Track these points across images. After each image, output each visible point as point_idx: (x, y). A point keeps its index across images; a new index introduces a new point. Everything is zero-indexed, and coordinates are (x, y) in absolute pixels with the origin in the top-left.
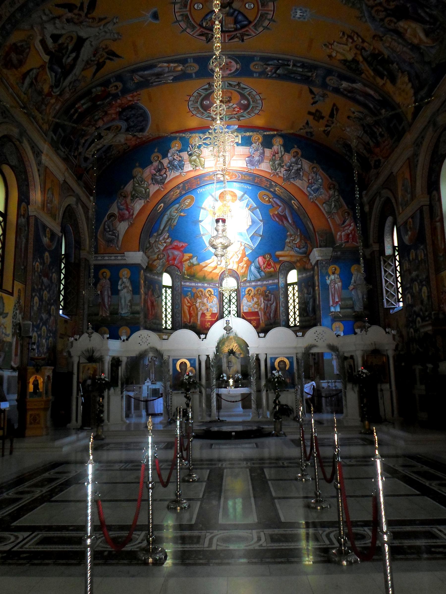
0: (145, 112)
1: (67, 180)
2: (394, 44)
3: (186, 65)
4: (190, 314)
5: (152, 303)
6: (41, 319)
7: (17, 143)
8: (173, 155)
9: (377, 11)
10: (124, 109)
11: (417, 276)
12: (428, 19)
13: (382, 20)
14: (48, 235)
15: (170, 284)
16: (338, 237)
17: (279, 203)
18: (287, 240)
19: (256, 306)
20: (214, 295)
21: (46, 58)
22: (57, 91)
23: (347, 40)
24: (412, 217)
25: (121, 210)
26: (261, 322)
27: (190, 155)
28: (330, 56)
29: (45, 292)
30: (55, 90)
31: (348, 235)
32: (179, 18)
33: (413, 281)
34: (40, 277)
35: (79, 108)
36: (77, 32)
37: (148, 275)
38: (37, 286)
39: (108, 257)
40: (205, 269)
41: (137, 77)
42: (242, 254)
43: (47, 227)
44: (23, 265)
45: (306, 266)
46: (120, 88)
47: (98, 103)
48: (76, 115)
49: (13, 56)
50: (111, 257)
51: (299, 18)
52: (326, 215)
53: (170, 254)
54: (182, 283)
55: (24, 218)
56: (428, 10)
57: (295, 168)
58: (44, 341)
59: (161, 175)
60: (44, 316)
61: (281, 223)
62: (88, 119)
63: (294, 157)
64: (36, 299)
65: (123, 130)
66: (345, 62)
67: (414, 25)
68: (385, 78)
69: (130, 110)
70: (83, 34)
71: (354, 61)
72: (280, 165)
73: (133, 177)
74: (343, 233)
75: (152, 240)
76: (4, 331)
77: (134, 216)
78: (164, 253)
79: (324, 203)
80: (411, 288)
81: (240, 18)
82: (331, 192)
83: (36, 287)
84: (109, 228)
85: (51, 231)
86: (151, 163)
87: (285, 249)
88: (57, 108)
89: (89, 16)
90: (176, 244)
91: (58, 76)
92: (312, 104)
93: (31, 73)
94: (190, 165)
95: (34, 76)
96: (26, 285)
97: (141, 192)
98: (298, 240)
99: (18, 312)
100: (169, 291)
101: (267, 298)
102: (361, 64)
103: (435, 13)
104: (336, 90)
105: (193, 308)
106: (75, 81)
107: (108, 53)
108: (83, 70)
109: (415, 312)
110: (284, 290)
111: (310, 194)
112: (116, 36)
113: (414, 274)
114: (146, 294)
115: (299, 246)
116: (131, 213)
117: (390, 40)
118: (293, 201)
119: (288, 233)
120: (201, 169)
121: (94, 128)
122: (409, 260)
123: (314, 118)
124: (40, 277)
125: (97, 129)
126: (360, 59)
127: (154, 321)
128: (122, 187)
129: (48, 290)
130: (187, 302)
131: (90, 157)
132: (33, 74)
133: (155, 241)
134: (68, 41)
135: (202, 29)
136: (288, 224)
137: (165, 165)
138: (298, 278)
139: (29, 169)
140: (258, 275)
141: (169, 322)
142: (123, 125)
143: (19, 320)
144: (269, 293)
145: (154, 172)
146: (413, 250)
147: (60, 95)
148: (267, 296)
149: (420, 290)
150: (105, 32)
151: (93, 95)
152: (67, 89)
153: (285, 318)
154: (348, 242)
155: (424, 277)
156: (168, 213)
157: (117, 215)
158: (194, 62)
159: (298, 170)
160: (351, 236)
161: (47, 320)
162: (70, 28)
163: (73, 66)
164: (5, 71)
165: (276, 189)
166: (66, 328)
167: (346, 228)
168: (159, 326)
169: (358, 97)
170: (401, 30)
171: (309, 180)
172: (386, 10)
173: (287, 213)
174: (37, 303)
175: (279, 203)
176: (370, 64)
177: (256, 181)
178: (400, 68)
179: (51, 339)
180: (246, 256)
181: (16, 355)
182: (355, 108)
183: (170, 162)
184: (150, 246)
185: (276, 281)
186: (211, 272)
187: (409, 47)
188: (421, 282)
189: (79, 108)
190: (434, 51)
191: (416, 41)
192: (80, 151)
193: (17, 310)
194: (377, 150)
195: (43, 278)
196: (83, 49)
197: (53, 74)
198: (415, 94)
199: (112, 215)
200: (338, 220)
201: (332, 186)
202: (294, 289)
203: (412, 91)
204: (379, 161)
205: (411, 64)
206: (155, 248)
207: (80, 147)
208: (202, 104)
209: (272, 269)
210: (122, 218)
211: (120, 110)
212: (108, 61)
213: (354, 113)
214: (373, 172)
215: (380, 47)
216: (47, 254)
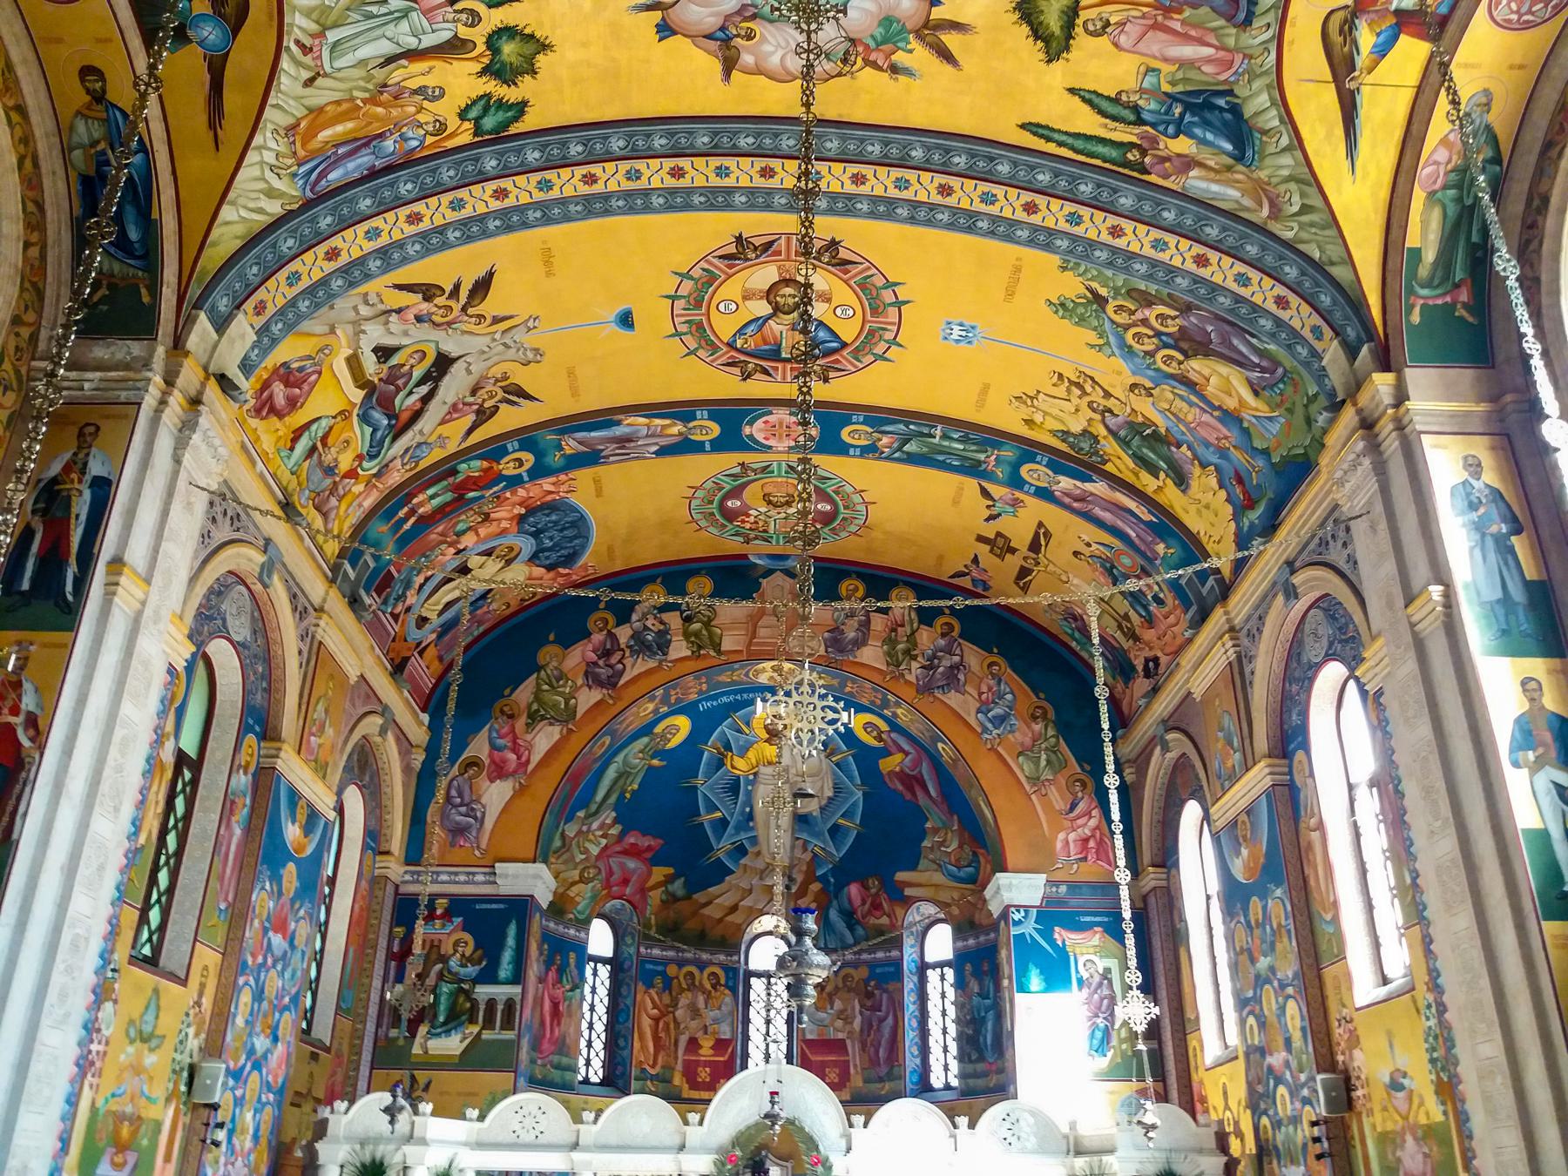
0: (582, 518)
1: (368, 676)
2: (1178, 403)
3: (691, 425)
4: (656, 1039)
5: (555, 1005)
6: (251, 1052)
7: (258, 587)
8: (644, 617)
9: (1138, 337)
10: (531, 511)
11: (1272, 969)
12: (1256, 360)
13: (1151, 354)
14: (302, 815)
15: (608, 951)
16: (1059, 845)
17: (906, 747)
18: (926, 843)
19: (839, 1023)
20: (726, 986)
21: (357, 395)
22: (371, 467)
23: (1068, 391)
24: (1249, 811)
25: (499, 749)
26: (852, 1071)
27: (688, 620)
28: (1029, 422)
29: (273, 973)
30: (366, 464)
31: (1086, 840)
32: (683, 328)
33: (1260, 981)
34: (265, 931)
35: (421, 504)
36: (437, 343)
37: (552, 925)
38: (254, 956)
39: (450, 873)
40: (706, 911)
41: (572, 442)
42: (806, 873)
43: (301, 797)
44: (226, 899)
45: (977, 916)
46: (527, 466)
47: (471, 495)
48: (413, 520)
49: (279, 392)
50: (456, 874)
51: (957, 341)
52: (1027, 787)
53: (615, 868)
54: (642, 950)
55: (245, 773)
56: (1254, 341)
57: (946, 663)
58: (249, 1116)
59: (611, 666)
60: (261, 1043)
61: (908, 796)
62: (440, 529)
63: (943, 635)
64: (246, 997)
65: (526, 554)
66: (1065, 435)
67: (1224, 369)
68: (1162, 475)
70: (451, 347)
71: (1085, 432)
72: (907, 652)
73: (539, 668)
74: (1072, 836)
75: (571, 830)
76: (145, 1088)
77: (531, 767)
78: (601, 865)
79: (1020, 754)
80: (1257, 999)
81: (822, 334)
82: (1038, 727)
83: (250, 961)
84: (460, 795)
85: (310, 805)
86: (588, 635)
87: (920, 867)
88: (368, 503)
89: (471, 311)
90: (632, 840)
91: (379, 434)
92: (987, 520)
93: (314, 427)
94: (684, 643)
95: (320, 434)
97: (555, 705)
98: (955, 845)
99: (191, 1031)
100: (604, 971)
101: (869, 1003)
102: (1103, 442)
103: (1272, 347)
104: (1044, 494)
105: (667, 1025)
106: (419, 445)
107: (505, 390)
108: (443, 422)
109: (1270, 1069)
110: (915, 979)
111: (985, 730)
112: (530, 355)
113: (1263, 963)
114: (541, 980)
115: (958, 860)
116: (524, 759)
117: (1171, 396)
118: (940, 745)
119: (928, 825)
120: (712, 653)
121: (452, 551)
122: (1248, 923)
123: (991, 551)
124: (265, 931)
126: (1102, 431)
127: (556, 1058)
128: (507, 692)
129: (279, 967)
130: (649, 1005)
131: (433, 616)
132: (318, 430)
133: (580, 832)
134: (412, 361)
135: (733, 353)
136: (929, 802)
137: (623, 641)
138: (955, 950)
140: (847, 933)
141: (597, 1064)
142: (526, 545)
144: (877, 987)
145: (593, 657)
146: (1255, 898)
147: (378, 475)
148: (869, 995)
149: (1282, 1009)
150: (505, 345)
151: (460, 477)
152: (398, 462)
153: (918, 1061)
154: (1085, 859)
155: (1290, 974)
156: (620, 758)
157: (487, 762)
158: (710, 419)
159: (955, 668)
160: (1092, 844)
161: (265, 1056)
162: (424, 332)
163: (416, 415)
164: (254, 423)
165: (899, 711)
166: (311, 1075)
167: (1080, 822)
168: (568, 1075)
169: (1098, 512)
170: (1193, 376)
171: (980, 694)
172: (1158, 334)
173: (926, 770)
175: (906, 747)
176: (1125, 443)
177: (848, 689)
178: (1196, 457)
179: (268, 1109)
180: (819, 879)
181: (167, 1159)
182: (1090, 533)
183: (636, 636)
184: (564, 845)
185: (895, 953)
186: (720, 920)
187: (1216, 413)
188: (1283, 986)
189: (421, 504)
190: (1275, 428)
191: (1231, 404)
192: (408, 602)
193: (189, 1026)
194: (1149, 635)
195: (271, 934)
196: (447, 379)
197: (368, 430)
198: (1236, 517)
199: (473, 763)
200: (1058, 800)
201: (1039, 712)
202: (943, 978)
203: (1229, 509)
204: (1156, 660)
205: (1223, 453)
206: (576, 851)
208: (722, 507)
209: (885, 920)
210: (499, 771)
211: (523, 511)
212: (503, 407)
213: (1089, 545)
214: (1141, 685)
215: (1146, 408)
216: (291, 866)
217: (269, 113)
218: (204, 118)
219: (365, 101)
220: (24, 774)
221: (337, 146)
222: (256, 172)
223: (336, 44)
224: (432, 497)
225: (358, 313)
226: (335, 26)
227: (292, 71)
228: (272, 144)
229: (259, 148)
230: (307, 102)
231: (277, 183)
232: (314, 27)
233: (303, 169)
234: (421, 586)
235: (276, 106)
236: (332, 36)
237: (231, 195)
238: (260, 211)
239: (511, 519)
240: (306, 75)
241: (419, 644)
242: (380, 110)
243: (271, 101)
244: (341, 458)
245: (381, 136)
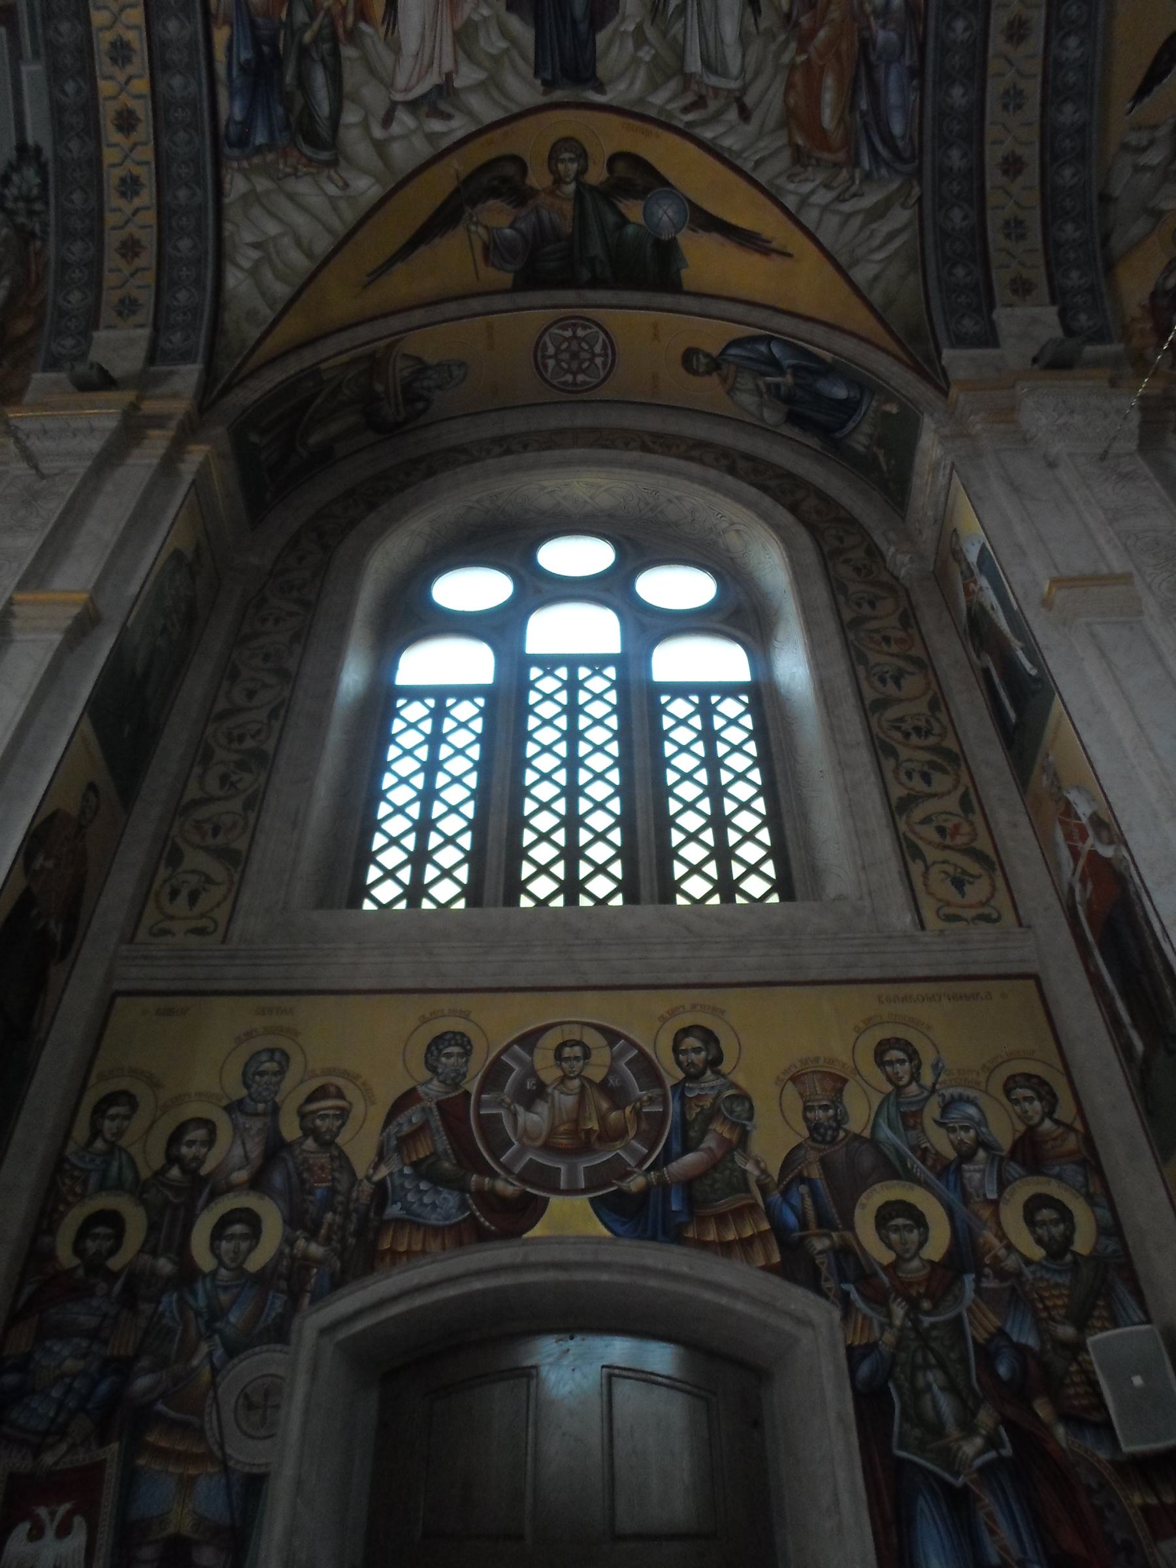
217: (762, 177)
218: (756, 259)
219: (801, 50)
220: (1132, 889)
221: (853, 106)
222: (833, 221)
223: (707, 64)
225: (1152, 169)
226: (681, 56)
227: (720, 129)
228: (807, 187)
229: (804, 201)
230: (771, 122)
231: (867, 202)
232: (673, 85)
233: (866, 163)
235: (758, 164)
236: (694, 64)
237: (843, 260)
238: (891, 237)
240: (732, 115)
242: (822, 34)
243: (748, 167)
245: (866, 44)
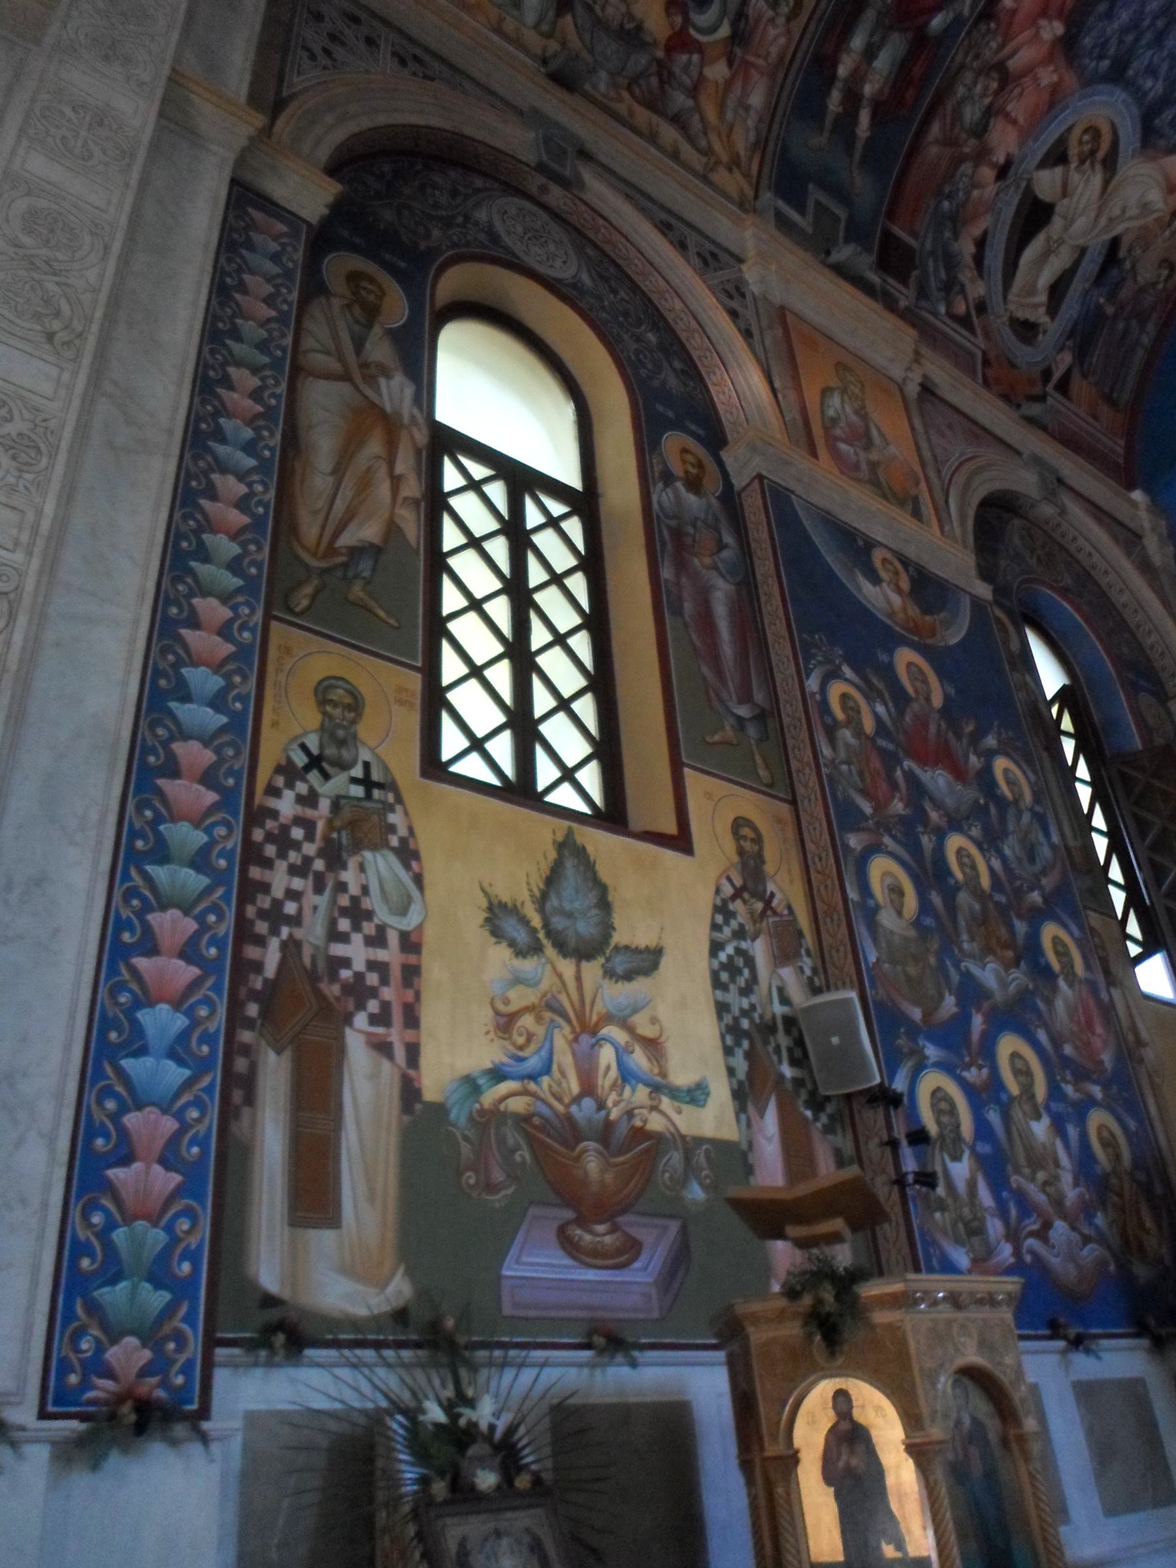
35: (857, 77)
47: (937, 22)
48: (864, 117)
65: (1129, 134)
69: (1102, 8)
88: (757, 99)
96: (793, 802)
99: (760, 949)
125: (1002, 172)
131: (1040, 316)
139: (671, 307)
143: (785, 1000)
147: (741, 36)
174: (896, 891)
179: (1097, 1118)
189: (857, 77)
207: (966, 275)
211: (1059, 28)
224: (870, 53)
234: (979, 259)
239: (1050, 58)
241: (1047, 374)
244: (638, 10)
